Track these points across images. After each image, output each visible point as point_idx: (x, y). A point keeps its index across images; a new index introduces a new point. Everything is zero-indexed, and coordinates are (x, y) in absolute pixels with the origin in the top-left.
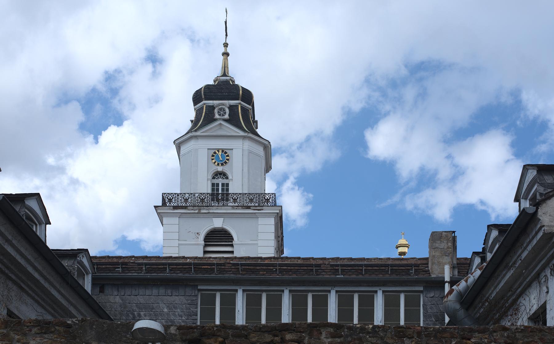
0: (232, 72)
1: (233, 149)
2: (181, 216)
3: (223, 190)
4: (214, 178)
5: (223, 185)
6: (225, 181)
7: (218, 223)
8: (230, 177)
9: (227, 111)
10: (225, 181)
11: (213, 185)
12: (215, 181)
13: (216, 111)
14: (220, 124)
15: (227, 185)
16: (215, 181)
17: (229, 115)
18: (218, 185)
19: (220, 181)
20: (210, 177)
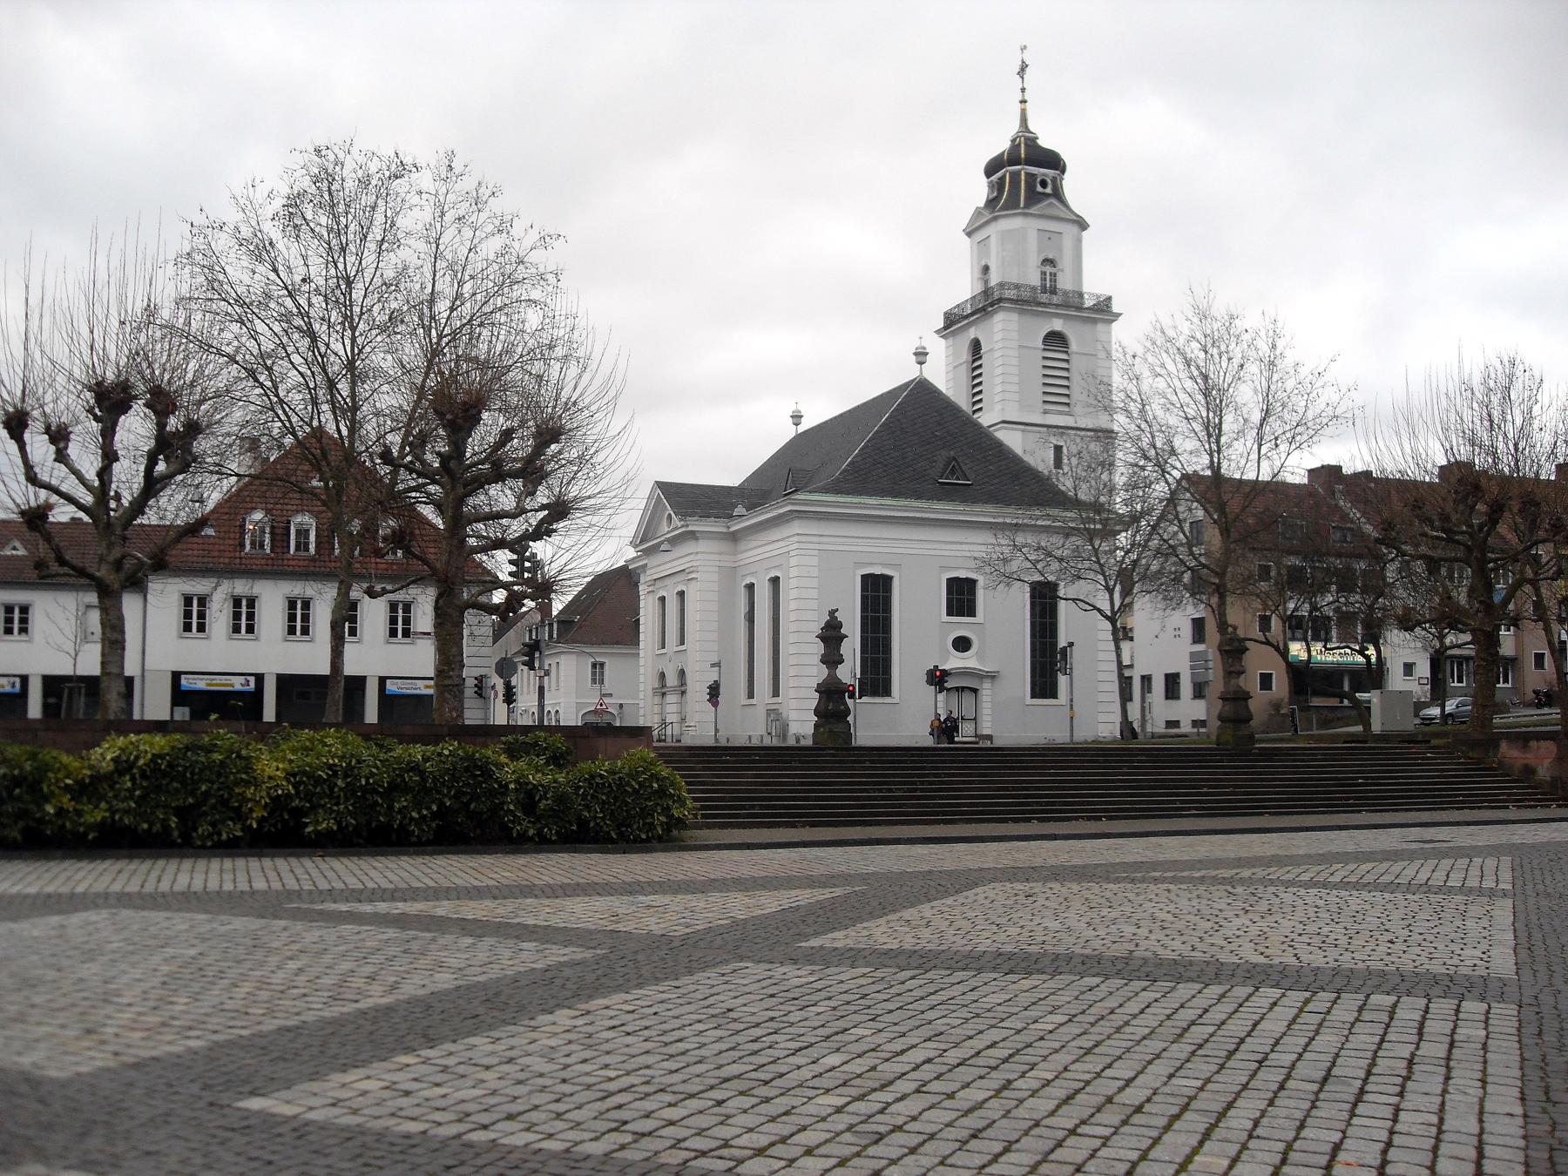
0: (1031, 127)
2: (1022, 312)
6: (1053, 270)
7: (1057, 325)
10: (1053, 270)
12: (1044, 269)
14: (1051, 203)
15: (1055, 275)
16: (1044, 269)
18: (1045, 273)
19: (1048, 269)
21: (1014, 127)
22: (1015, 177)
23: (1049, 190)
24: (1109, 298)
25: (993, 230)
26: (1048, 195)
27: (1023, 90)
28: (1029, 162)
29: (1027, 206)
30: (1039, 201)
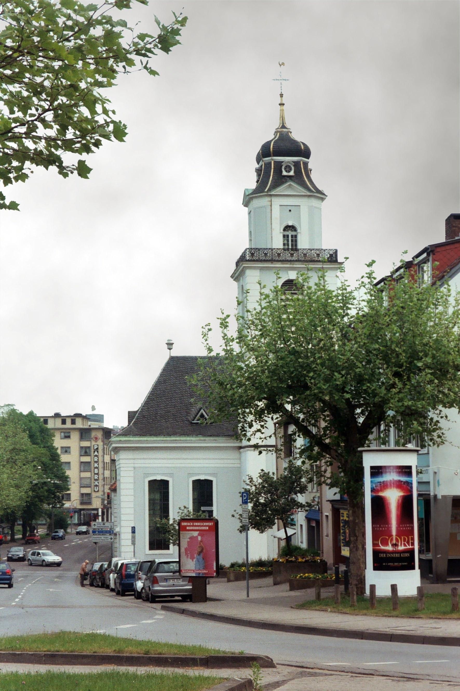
1: (300, 206)
3: (292, 241)
4: (284, 230)
5: (292, 236)
6: (294, 233)
7: (292, 275)
8: (299, 231)
9: (293, 168)
10: (294, 233)
11: (284, 236)
12: (286, 233)
13: (283, 167)
14: (290, 185)
15: (296, 236)
16: (286, 233)
17: (295, 172)
18: (288, 236)
19: (290, 233)
20: (282, 231)
21: (277, 124)
22: (268, 165)
23: (292, 173)
24: (336, 252)
25: (256, 203)
26: (290, 177)
27: (281, 95)
28: (278, 153)
29: (270, 190)
30: (282, 183)
